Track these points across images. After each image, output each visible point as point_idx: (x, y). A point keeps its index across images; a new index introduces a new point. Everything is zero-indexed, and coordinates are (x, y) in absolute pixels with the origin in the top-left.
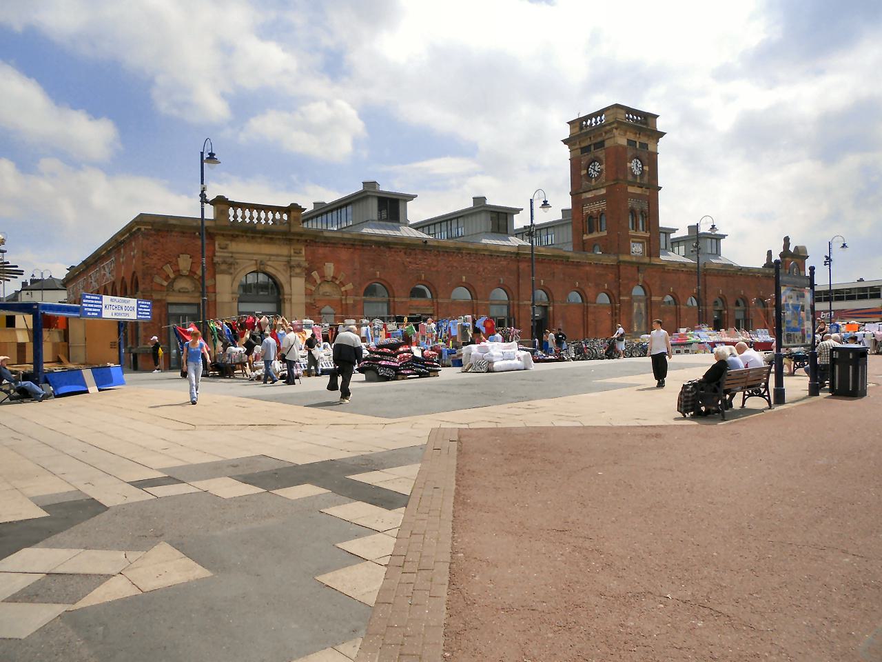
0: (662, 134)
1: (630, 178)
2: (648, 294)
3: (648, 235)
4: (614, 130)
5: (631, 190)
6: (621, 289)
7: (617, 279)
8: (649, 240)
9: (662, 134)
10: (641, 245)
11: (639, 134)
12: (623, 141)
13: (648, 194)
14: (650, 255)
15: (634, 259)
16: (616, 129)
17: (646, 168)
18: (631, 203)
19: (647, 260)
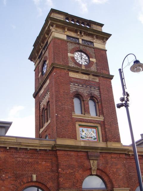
0: (109, 36)
1: (72, 65)
2: (109, 185)
3: (101, 119)
4: (51, 28)
5: (72, 75)
6: (61, 180)
7: (55, 168)
8: (103, 124)
9: (109, 36)
10: (94, 130)
11: (81, 33)
12: (64, 37)
13: (97, 81)
14: (106, 140)
15: (82, 144)
16: (52, 26)
17: (94, 60)
18: (73, 88)
19: (102, 145)
